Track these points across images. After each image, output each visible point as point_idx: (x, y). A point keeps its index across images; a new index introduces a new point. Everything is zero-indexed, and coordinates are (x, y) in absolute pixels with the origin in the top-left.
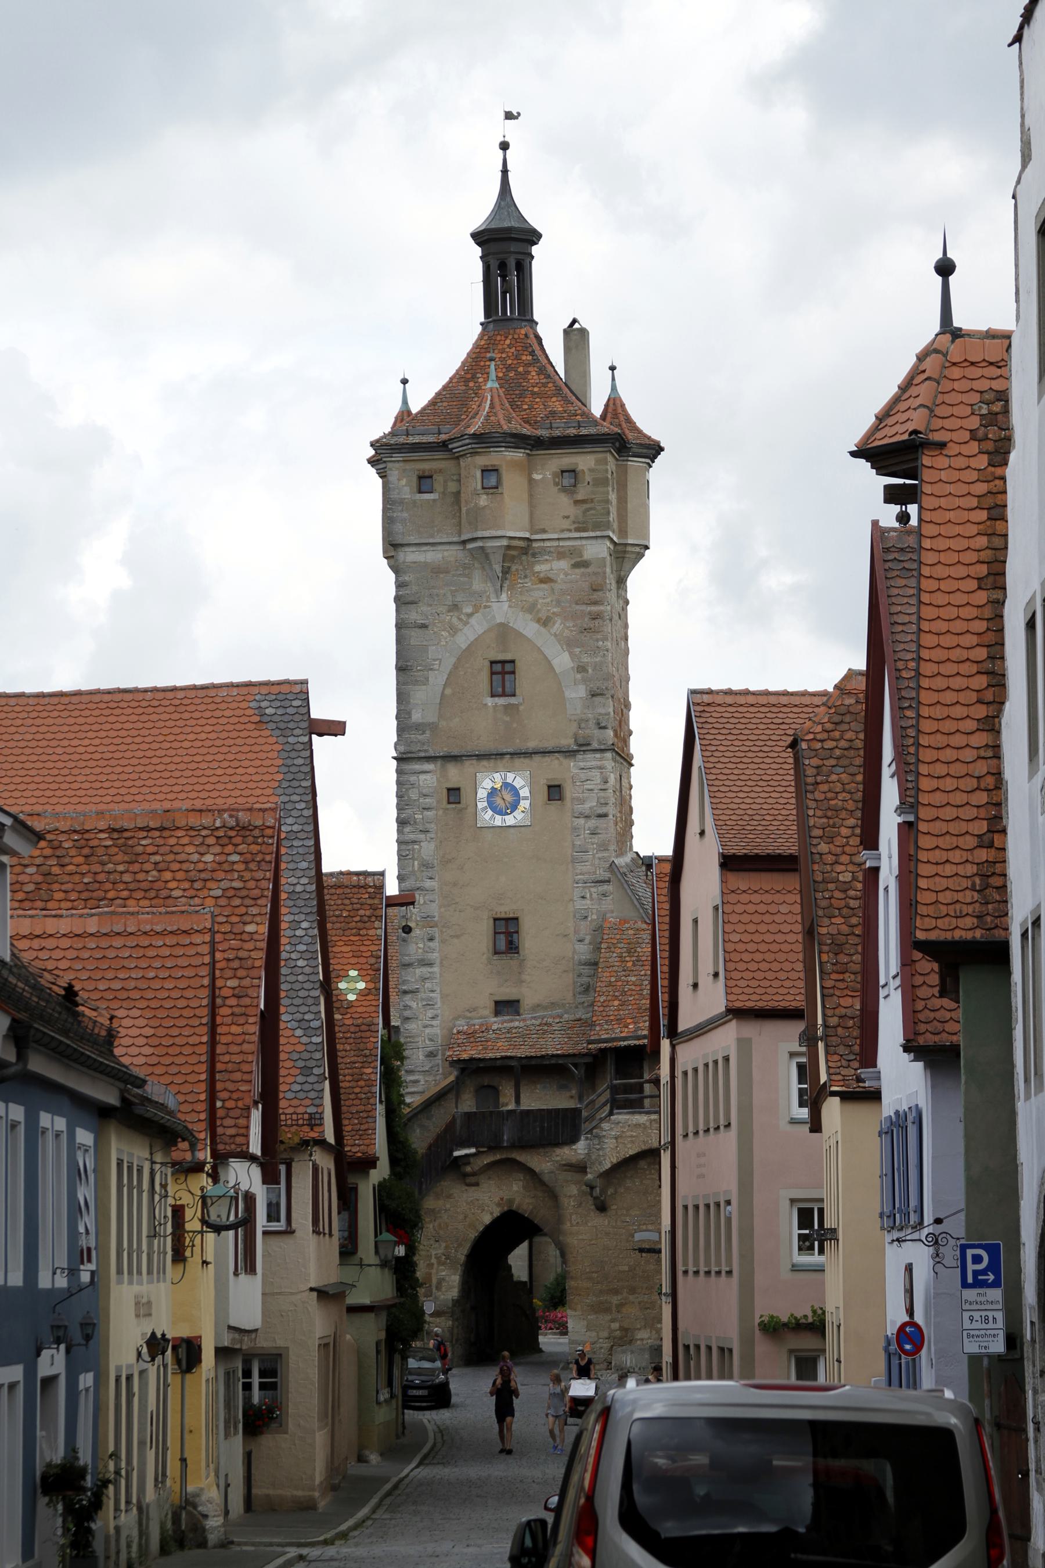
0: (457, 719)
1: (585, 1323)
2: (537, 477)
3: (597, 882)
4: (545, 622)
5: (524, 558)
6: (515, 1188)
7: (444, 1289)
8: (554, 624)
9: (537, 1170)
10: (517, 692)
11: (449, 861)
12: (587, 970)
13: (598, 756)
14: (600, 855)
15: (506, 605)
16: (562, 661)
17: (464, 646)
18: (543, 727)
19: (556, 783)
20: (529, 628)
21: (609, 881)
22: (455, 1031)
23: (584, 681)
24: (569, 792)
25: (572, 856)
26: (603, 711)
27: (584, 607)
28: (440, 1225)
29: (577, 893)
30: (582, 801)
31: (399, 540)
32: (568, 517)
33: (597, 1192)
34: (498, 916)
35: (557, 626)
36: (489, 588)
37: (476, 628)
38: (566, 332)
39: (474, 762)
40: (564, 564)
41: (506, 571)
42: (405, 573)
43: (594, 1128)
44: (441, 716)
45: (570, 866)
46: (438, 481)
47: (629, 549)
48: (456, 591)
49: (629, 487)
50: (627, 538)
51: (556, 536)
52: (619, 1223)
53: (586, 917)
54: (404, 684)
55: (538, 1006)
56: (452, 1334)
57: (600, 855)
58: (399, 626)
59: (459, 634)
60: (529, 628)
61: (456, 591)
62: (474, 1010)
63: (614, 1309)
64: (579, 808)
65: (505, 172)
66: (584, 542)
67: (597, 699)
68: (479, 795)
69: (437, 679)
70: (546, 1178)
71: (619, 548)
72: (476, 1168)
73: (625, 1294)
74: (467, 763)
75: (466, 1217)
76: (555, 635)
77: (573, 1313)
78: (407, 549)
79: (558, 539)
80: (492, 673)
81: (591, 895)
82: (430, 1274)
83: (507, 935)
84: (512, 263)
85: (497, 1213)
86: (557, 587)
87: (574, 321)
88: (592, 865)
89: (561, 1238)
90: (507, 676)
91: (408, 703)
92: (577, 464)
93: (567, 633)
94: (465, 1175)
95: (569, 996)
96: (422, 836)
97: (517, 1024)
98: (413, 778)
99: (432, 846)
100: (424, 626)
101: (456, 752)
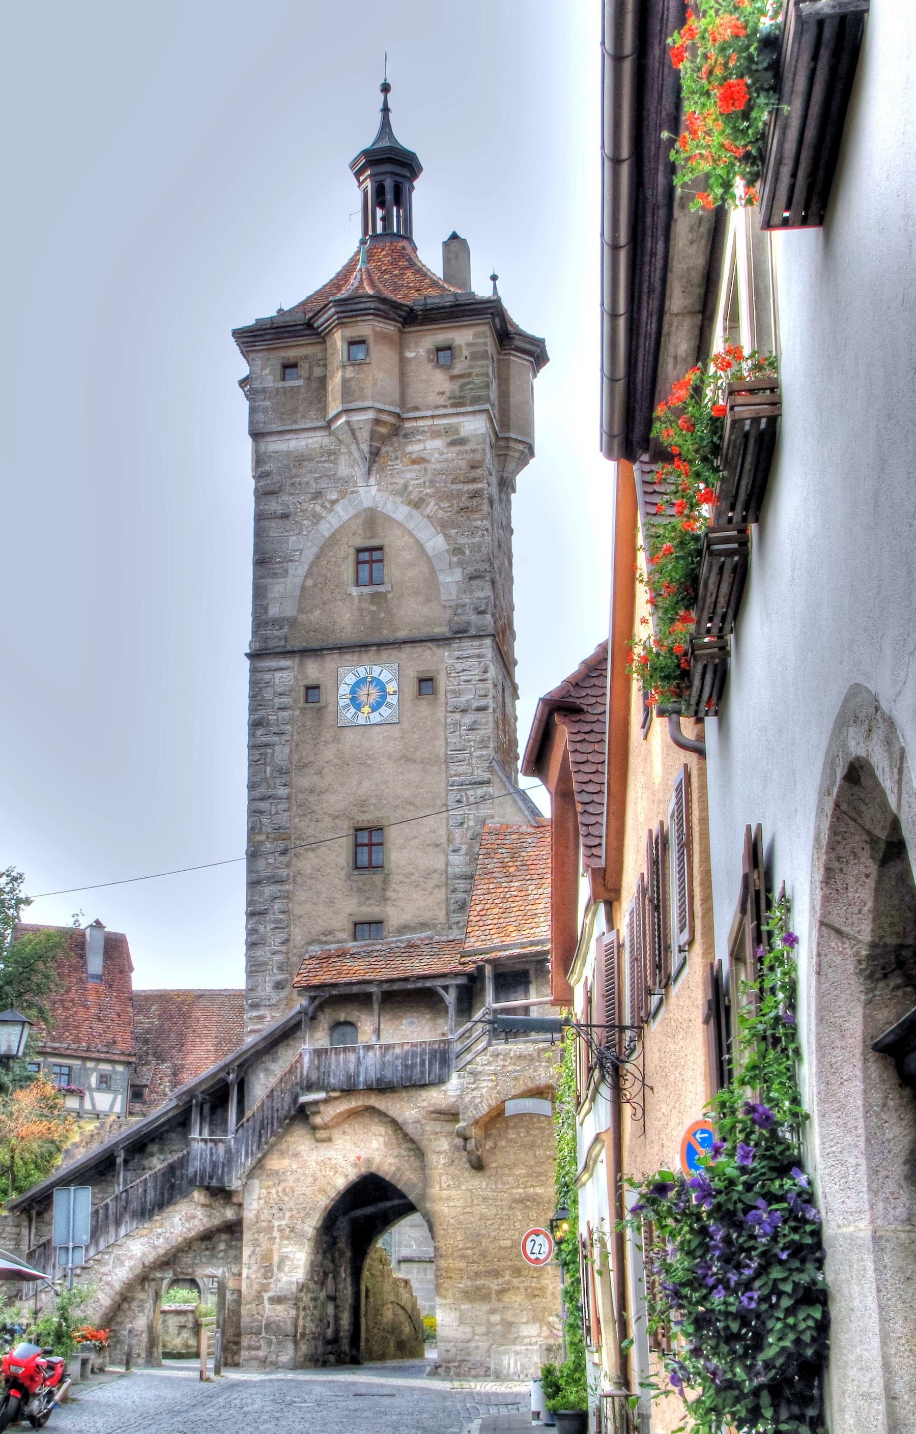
0: (318, 612)
1: (458, 1314)
2: (410, 355)
3: (475, 783)
4: (417, 504)
5: (395, 439)
6: (375, 1145)
7: (287, 1269)
8: (427, 505)
9: (400, 1120)
10: (386, 579)
11: (305, 766)
12: (462, 885)
13: (476, 643)
14: (478, 753)
15: (374, 490)
16: (436, 543)
17: (327, 534)
18: (412, 613)
19: (428, 675)
20: (400, 511)
21: (488, 782)
22: (307, 957)
23: (460, 564)
24: (442, 683)
25: (446, 755)
26: (481, 594)
27: (460, 486)
28: (284, 1190)
29: (452, 797)
30: (457, 694)
31: (261, 428)
32: (442, 393)
33: (471, 1145)
34: (361, 825)
35: (431, 507)
36: (359, 472)
37: (342, 513)
38: (445, 244)
39: (336, 656)
40: (438, 443)
41: (375, 454)
42: (265, 463)
43: (469, 1063)
44: (301, 610)
45: (443, 767)
46: (303, 371)
47: (512, 444)
48: (320, 478)
49: (512, 381)
50: (508, 430)
51: (430, 413)
52: (499, 1186)
53: (462, 824)
54: (261, 578)
55: (406, 927)
56: (296, 1327)
57: (478, 753)
58: (260, 517)
59: (323, 522)
60: (400, 511)
61: (320, 478)
62: (330, 933)
63: (494, 1296)
64: (452, 701)
65: (386, 110)
66: (461, 419)
67: (474, 582)
68: (341, 692)
69: (297, 572)
70: (410, 1130)
71: (502, 443)
72: (327, 1119)
73: (507, 1278)
74: (328, 658)
75: (315, 1180)
76: (429, 517)
77: (444, 1301)
78: (269, 439)
79: (433, 417)
80: (359, 563)
81: (467, 798)
82: (271, 1251)
83: (368, 846)
84: (389, 184)
85: (352, 1174)
86: (430, 467)
87: (454, 236)
88: (469, 764)
89: (428, 1205)
90: (374, 565)
91: (265, 597)
92: (453, 339)
93: (441, 514)
94: (314, 1128)
95: (441, 916)
96: (276, 739)
97: (379, 947)
98: (267, 676)
99: (287, 750)
100: (285, 516)
101: (316, 645)
